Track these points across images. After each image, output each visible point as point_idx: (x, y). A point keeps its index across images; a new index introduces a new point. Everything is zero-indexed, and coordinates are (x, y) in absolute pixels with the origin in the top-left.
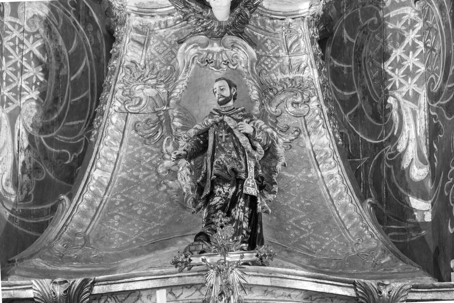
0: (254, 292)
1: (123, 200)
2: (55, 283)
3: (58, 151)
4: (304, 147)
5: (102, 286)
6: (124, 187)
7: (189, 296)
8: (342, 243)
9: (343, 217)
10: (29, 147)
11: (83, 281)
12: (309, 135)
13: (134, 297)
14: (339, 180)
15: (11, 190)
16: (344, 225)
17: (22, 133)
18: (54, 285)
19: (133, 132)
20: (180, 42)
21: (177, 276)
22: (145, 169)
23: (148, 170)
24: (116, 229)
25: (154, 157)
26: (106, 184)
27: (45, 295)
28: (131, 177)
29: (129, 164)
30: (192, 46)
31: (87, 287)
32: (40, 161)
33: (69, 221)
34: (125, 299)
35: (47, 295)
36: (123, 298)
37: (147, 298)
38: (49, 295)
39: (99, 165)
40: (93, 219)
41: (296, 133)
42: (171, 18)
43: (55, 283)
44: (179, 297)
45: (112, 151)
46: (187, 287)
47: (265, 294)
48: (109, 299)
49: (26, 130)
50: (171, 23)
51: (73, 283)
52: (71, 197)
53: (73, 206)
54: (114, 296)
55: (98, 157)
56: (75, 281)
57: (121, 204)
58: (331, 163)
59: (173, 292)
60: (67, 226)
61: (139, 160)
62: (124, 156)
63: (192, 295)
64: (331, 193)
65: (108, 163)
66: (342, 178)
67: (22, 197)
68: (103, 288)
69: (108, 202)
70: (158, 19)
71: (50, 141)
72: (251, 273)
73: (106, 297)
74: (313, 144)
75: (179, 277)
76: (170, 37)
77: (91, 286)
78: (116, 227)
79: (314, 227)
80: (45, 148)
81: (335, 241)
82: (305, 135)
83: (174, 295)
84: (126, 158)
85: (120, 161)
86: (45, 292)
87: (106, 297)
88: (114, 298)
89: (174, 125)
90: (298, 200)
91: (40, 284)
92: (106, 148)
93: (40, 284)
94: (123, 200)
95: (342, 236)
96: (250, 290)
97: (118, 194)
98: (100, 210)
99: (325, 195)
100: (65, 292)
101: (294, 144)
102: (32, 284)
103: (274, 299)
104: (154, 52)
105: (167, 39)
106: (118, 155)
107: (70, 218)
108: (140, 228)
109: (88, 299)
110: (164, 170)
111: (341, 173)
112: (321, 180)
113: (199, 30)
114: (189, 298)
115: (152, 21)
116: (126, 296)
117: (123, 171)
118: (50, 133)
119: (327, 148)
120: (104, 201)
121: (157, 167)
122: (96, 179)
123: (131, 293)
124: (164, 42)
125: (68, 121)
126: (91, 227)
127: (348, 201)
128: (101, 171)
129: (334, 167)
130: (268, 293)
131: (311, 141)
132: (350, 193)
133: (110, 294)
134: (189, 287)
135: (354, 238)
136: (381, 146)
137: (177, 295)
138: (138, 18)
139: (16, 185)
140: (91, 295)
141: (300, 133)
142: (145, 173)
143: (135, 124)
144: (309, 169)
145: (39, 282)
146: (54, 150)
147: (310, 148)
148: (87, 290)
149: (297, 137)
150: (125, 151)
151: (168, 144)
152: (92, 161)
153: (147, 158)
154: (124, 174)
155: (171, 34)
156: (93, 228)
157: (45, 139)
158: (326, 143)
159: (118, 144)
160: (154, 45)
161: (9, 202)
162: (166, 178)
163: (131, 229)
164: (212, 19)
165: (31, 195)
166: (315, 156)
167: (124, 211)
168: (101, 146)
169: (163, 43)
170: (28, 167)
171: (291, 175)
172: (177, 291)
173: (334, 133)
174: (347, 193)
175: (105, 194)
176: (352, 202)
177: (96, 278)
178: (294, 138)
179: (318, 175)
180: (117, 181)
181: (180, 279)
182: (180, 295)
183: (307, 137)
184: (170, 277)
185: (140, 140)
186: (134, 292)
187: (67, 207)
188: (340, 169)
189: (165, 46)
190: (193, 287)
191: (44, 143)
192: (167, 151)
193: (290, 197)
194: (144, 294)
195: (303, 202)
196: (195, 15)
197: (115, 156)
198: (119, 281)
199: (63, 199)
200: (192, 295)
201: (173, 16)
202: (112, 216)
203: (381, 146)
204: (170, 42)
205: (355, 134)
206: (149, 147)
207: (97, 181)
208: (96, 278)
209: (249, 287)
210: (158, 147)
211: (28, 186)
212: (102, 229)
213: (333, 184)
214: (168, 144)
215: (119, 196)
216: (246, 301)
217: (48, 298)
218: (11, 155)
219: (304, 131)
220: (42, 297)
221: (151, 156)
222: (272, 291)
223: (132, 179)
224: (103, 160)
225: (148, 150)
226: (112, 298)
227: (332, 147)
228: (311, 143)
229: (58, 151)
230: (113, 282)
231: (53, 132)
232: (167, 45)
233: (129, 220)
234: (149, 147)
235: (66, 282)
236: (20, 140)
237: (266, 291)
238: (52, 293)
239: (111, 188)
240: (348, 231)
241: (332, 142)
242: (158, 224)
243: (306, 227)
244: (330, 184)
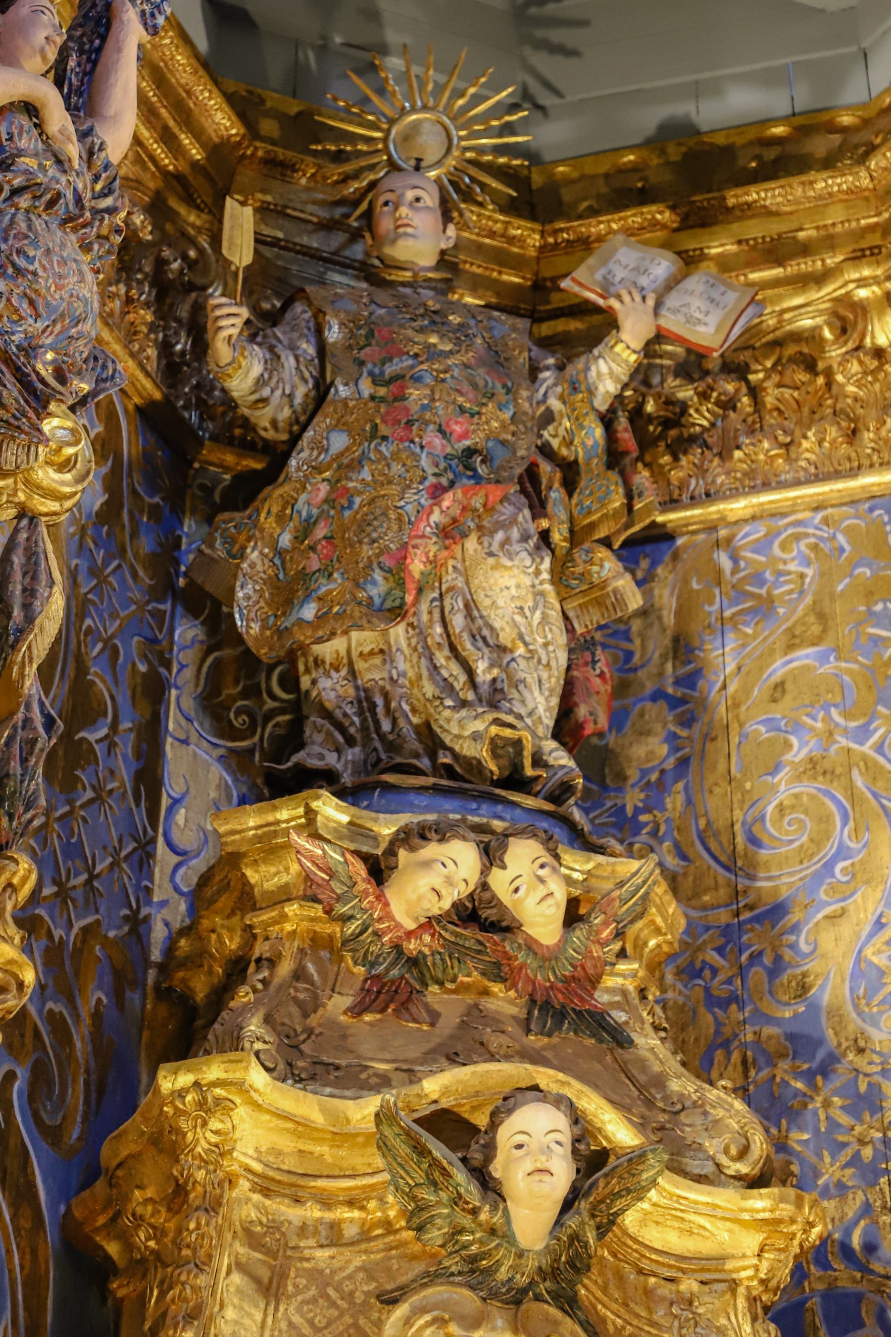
20: (390, 1300)
30: (428, 1317)
42: (356, 1214)
50: (350, 1232)
70: (313, 1212)
76: (349, 1277)
104: (297, 1319)
105: (341, 1283)
113: (454, 1269)
115: (294, 1214)
124: (331, 1292)
138: (256, 1197)
155: (351, 1268)
160: (299, 1298)
164: (504, 1236)
169: (328, 1296)
189: (333, 1304)
196: (448, 1216)
201: (362, 1208)
204: (352, 1294)
232: (339, 1302)
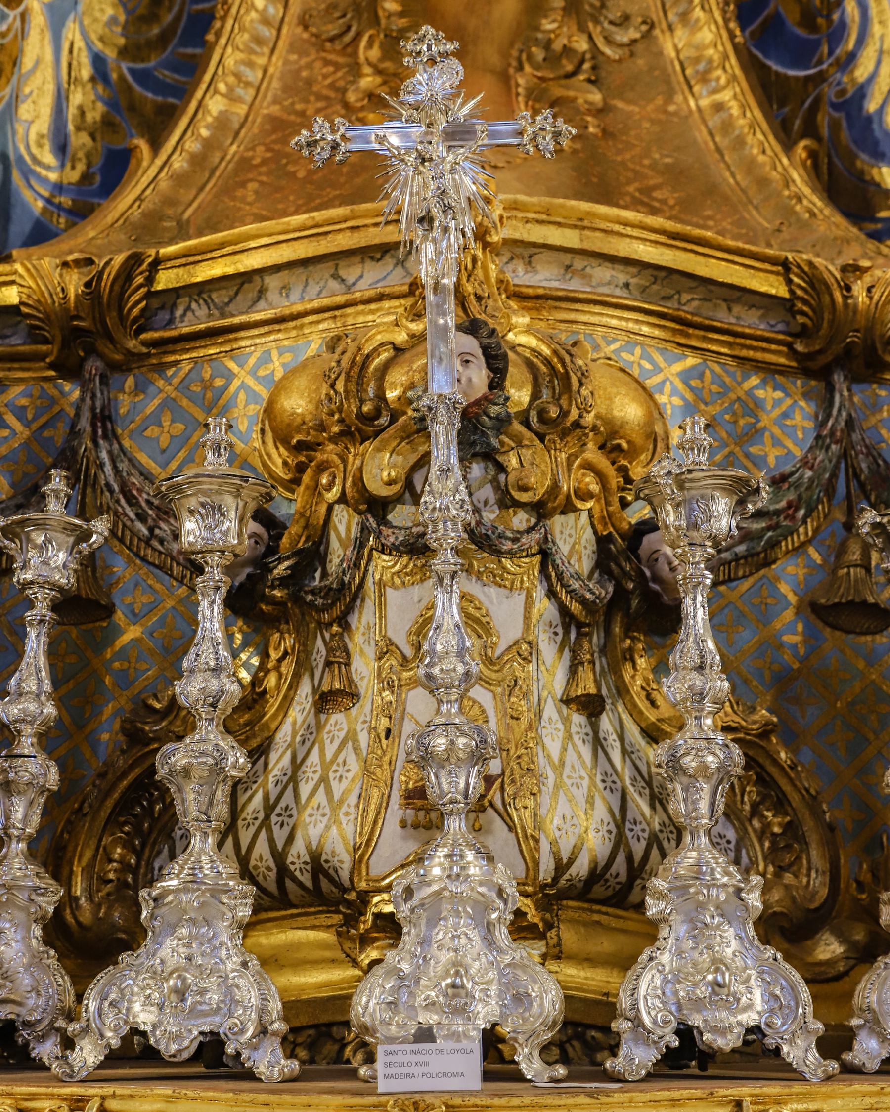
0: (539, 268)
1: (269, 155)
2: (65, 264)
3: (160, 99)
4: (661, 53)
5: (175, 271)
6: (274, 131)
7: (377, 282)
8: (744, 231)
9: (743, 184)
10: (92, 79)
11: (130, 258)
12: (671, 28)
13: (250, 295)
14: (735, 111)
15: (49, 158)
16: (747, 197)
17: (80, 49)
18: (64, 271)
19: (299, 30)
21: (348, 228)
22: (319, 97)
23: (327, 98)
24: (248, 207)
25: (339, 74)
26: (236, 126)
27: (42, 293)
28: (289, 114)
29: (287, 89)
31: (141, 273)
32: (119, 112)
33: (148, 192)
34: (231, 301)
35: (47, 295)
36: (226, 300)
37: (281, 293)
38: (51, 295)
39: (222, 87)
40: (201, 189)
41: (644, 28)
43: (65, 264)
44: (354, 284)
45: (251, 64)
46: (372, 258)
47: (568, 276)
48: (194, 305)
49: (87, 44)
51: (107, 264)
52: (156, 146)
53: (159, 162)
54: (205, 296)
55: (220, 71)
56: (111, 260)
57: (264, 162)
58: (718, 79)
59: (342, 273)
60: (142, 201)
61: (309, 82)
62: (278, 74)
63: (385, 277)
64: (718, 139)
65: (242, 85)
66: (743, 107)
67: (73, 176)
68: (178, 275)
69: (236, 158)
71: (143, 77)
72: (531, 215)
73: (187, 299)
74: (680, 46)
75: (353, 228)
77: (150, 271)
78: (250, 204)
79: (680, 202)
80: (129, 88)
81: (729, 227)
82: (662, 31)
83: (343, 280)
84: (281, 79)
85: (269, 83)
86: (43, 288)
87: (187, 299)
88: (205, 300)
89: (384, 10)
90: (646, 153)
91: (32, 270)
92: (240, 56)
93: (32, 270)
94: (269, 155)
95: (743, 218)
96: (530, 263)
97: (259, 144)
98: (217, 174)
99: (706, 143)
100: (88, 285)
101: (639, 47)
102: (16, 272)
103: (588, 290)
106: (265, 71)
107: (152, 187)
108: (300, 202)
109: (144, 303)
110: (361, 96)
111: (740, 97)
112: (696, 115)
114: (379, 285)
116: (232, 293)
117: (275, 102)
118: (143, 61)
119: (711, 52)
120: (228, 157)
121: (344, 91)
122: (215, 113)
123: (242, 284)
125: (184, 43)
126: (195, 205)
127: (755, 151)
128: (225, 101)
129: (724, 88)
130: (573, 273)
131: (676, 40)
132: (760, 136)
133: (195, 290)
134: (378, 256)
135: (769, 223)
136: (821, 78)
137: (351, 280)
139: (62, 148)
140: (149, 295)
141: (652, 26)
142: (320, 105)
143: (305, 13)
144: (669, 97)
145: (29, 266)
146: (150, 95)
147: (673, 54)
148: (140, 280)
149: (646, 35)
150: (280, 63)
151: (370, 45)
152: (207, 77)
153: (325, 77)
154: (275, 109)
156: (199, 207)
157: (132, 71)
158: (707, 41)
159: (266, 51)
161: (44, 181)
162: (362, 108)
163: (280, 206)
165: (94, 174)
166: (683, 70)
167: (268, 174)
168: (229, 50)
170: (89, 117)
171: (631, 108)
172: (351, 270)
173: (726, 21)
174: (754, 134)
175: (232, 144)
176: (764, 152)
177: (162, 251)
178: (637, 35)
179: (688, 105)
180: (259, 120)
181: (356, 235)
182: (357, 281)
183: (668, 34)
184: (330, 232)
185: (314, 45)
186: (250, 282)
187: (145, 164)
188: (738, 90)
190: (388, 256)
191: (129, 78)
192: (367, 59)
193: (629, 146)
194: (273, 282)
195: (657, 156)
197: (260, 74)
198: (214, 254)
199: (137, 147)
200: (385, 277)
202: (243, 184)
203: (821, 78)
205: (764, 67)
206: (331, 57)
207: (216, 119)
208: (162, 251)
209: (526, 253)
210: (350, 56)
211: (88, 155)
212: (219, 208)
213: (723, 122)
214: (370, 45)
215: (260, 149)
216: (517, 289)
217: (50, 301)
218: (50, 87)
219: (660, 22)
220: (39, 301)
221: (335, 72)
222: (583, 269)
223: (293, 118)
224: (231, 79)
225: (327, 63)
226: (201, 302)
227: (720, 48)
228: (675, 46)
229: (160, 99)
230: (199, 258)
231: (149, 61)
233: (279, 189)
234: (331, 57)
235: (90, 262)
236: (75, 63)
237: (568, 267)
238: (59, 289)
239: (247, 133)
240: (756, 208)
241: (721, 37)
242: (338, 192)
243: (664, 202)
244: (714, 121)
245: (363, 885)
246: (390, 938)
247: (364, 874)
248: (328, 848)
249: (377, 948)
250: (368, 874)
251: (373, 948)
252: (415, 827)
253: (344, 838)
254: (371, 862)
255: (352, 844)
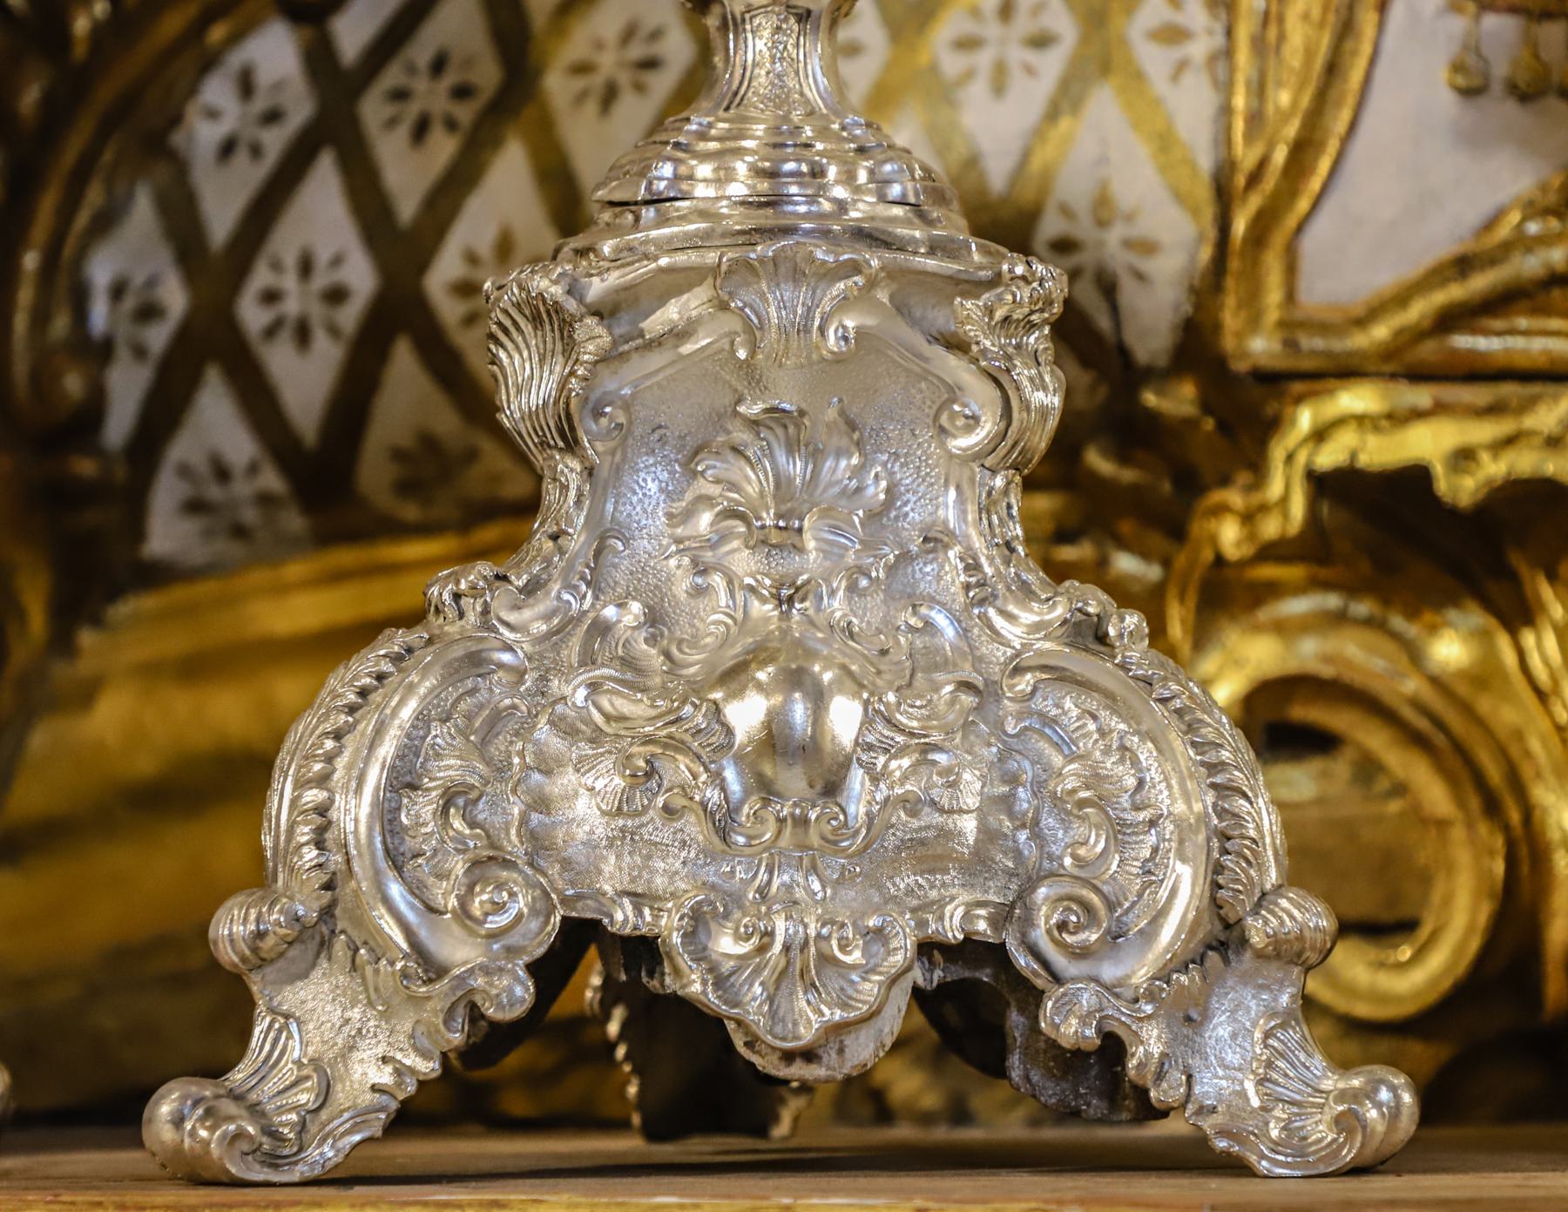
245: (1262, 347)
246: (1326, 586)
247: (1273, 296)
248: (1073, 187)
249: (1281, 628)
250: (1290, 296)
251: (1258, 629)
252: (1524, 94)
253: (1165, 142)
254: (1311, 243)
255: (1205, 162)
